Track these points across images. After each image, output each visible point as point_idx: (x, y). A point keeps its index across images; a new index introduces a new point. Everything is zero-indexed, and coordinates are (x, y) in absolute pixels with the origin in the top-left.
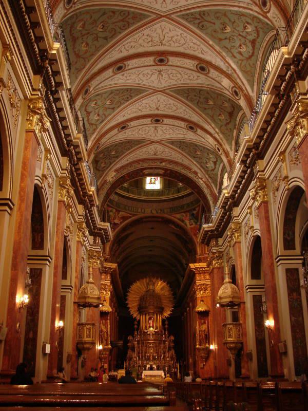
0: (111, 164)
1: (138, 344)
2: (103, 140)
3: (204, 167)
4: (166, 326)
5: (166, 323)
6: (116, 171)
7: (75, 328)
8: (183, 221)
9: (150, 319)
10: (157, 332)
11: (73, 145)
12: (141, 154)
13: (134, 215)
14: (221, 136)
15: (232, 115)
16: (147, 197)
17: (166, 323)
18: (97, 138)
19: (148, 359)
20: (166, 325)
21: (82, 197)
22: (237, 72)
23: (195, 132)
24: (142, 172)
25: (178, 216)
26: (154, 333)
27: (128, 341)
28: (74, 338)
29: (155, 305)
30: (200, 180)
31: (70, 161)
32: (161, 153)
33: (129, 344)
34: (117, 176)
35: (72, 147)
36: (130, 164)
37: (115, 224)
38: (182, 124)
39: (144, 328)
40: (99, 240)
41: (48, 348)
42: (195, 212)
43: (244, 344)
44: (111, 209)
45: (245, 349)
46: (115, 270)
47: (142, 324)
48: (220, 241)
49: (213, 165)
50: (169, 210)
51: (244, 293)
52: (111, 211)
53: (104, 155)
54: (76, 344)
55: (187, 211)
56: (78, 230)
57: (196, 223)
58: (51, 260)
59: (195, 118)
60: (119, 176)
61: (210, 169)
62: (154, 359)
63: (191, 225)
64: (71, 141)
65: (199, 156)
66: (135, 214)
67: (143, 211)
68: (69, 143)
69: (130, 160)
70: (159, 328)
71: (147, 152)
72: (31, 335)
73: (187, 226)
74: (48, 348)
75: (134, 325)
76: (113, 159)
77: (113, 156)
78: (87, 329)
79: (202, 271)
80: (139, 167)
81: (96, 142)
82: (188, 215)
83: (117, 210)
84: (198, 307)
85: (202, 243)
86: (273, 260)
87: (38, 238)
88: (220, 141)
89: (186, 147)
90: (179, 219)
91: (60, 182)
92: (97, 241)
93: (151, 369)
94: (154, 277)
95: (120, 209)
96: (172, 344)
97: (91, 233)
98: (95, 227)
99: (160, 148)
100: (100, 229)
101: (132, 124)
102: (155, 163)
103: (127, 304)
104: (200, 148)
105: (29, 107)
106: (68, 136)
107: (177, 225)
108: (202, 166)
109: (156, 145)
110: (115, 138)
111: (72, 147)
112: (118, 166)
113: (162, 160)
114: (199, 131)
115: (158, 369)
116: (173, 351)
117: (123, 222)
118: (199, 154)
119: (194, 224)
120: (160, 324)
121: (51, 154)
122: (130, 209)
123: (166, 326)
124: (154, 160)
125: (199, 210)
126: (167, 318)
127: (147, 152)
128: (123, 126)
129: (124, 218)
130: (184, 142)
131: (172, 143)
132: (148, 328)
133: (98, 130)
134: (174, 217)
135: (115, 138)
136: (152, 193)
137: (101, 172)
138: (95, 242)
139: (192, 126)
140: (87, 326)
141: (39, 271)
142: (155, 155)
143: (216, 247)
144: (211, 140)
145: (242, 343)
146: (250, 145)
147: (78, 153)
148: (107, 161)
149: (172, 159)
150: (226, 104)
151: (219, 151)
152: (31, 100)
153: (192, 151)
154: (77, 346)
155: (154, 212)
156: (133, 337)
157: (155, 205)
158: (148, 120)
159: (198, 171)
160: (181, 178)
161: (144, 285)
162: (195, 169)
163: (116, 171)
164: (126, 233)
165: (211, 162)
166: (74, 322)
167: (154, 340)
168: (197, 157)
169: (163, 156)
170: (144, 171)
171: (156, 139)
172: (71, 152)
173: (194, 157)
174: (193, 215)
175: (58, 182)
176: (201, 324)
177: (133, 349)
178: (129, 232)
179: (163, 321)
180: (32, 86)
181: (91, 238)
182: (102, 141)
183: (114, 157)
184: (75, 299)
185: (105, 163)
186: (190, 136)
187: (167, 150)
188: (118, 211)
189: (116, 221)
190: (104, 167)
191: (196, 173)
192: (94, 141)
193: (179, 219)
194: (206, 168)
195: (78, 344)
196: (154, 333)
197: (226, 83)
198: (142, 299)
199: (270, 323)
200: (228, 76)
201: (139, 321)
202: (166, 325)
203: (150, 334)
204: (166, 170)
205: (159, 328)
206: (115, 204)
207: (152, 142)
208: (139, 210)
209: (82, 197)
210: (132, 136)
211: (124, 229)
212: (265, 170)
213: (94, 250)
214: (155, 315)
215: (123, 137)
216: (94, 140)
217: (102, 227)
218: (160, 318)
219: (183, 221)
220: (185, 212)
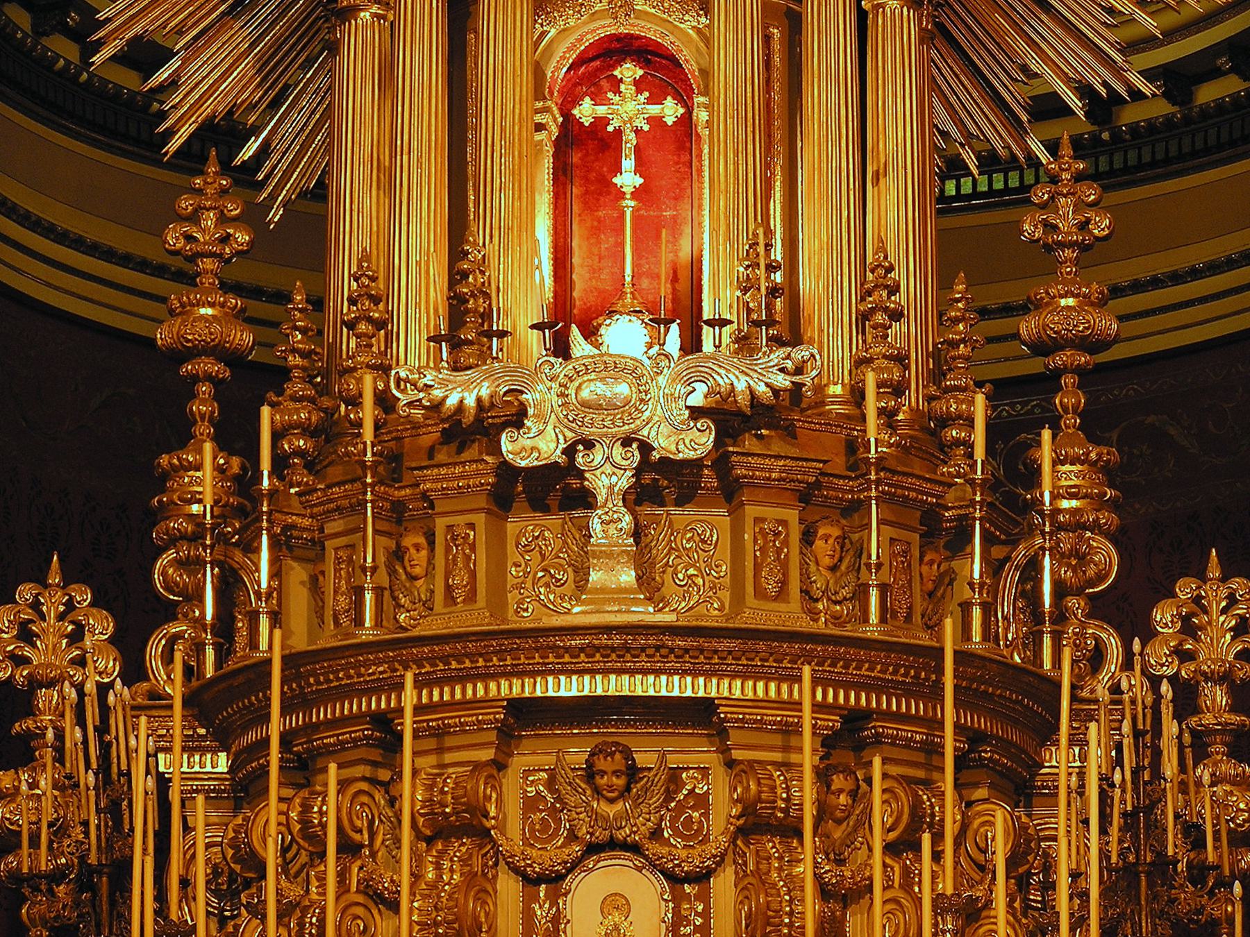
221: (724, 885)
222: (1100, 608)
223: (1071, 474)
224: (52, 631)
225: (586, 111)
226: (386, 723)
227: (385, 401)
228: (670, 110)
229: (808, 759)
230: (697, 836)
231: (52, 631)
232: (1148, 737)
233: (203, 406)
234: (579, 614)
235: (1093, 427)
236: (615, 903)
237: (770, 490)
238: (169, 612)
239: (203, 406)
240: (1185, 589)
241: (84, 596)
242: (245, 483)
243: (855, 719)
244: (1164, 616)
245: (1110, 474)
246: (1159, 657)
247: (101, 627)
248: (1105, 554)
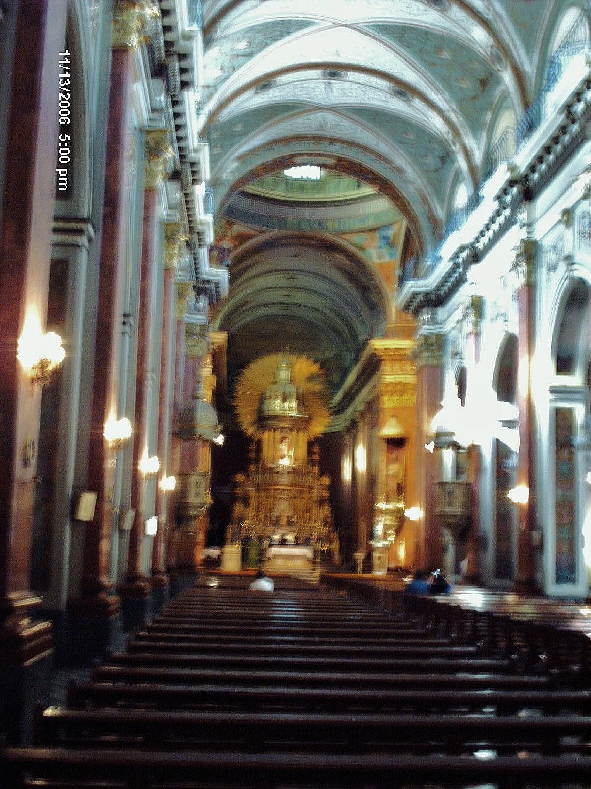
4: (316, 457)
8: (362, 249)
9: (282, 440)
15: (484, 83)
17: (316, 449)
19: (276, 523)
22: (505, 20)
23: (407, 101)
33: (239, 491)
38: (384, 84)
40: (203, 302)
47: (266, 452)
48: (441, 312)
57: (391, 255)
59: (410, 76)
62: (289, 523)
63: (379, 258)
75: (249, 451)
79: (398, 356)
84: (383, 424)
85: (407, 307)
93: (283, 543)
96: (326, 494)
99: (331, 118)
100: (208, 281)
101: (284, 78)
103: (233, 408)
110: (246, 104)
112: (246, 148)
113: (333, 140)
114: (417, 102)
115: (297, 543)
117: (241, 244)
120: (303, 451)
124: (318, 139)
125: (400, 229)
128: (264, 83)
135: (246, 104)
136: (303, 184)
139: (403, 89)
150: (477, 66)
158: (316, 73)
163: (242, 158)
164: (243, 265)
167: (292, 485)
174: (385, 238)
176: (389, 462)
177: (246, 501)
178: (248, 262)
179: (310, 444)
186: (397, 105)
191: (400, 170)
193: (354, 244)
197: (479, 35)
199: (519, 495)
200: (485, 23)
204: (340, 160)
207: (317, 108)
218: (303, 439)
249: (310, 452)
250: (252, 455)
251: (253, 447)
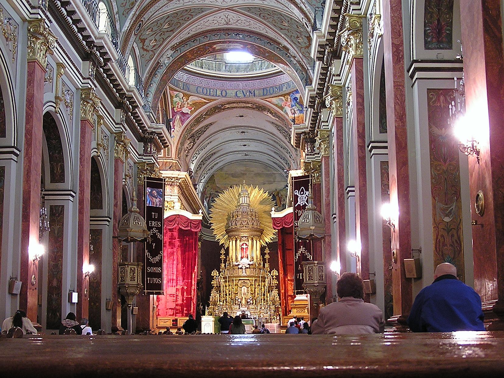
0: (164, 40)
1: (226, 282)
2: (146, 16)
3: (296, 43)
4: (267, 256)
5: (267, 251)
6: (173, 48)
7: (116, 269)
8: (282, 108)
10: (252, 265)
11: (96, 46)
12: (206, 24)
13: (210, 100)
14: (308, 8)
16: (229, 73)
17: (267, 251)
18: (137, 13)
20: (266, 254)
21: (119, 99)
24: (211, 47)
25: (274, 100)
26: (248, 266)
27: (212, 278)
28: (114, 282)
29: (250, 226)
30: (292, 59)
31: (94, 64)
32: (235, 21)
34: (176, 55)
35: (95, 49)
36: (194, 38)
37: (183, 114)
39: (234, 260)
41: (75, 296)
42: (298, 96)
43: (328, 288)
44: (176, 93)
45: (328, 292)
46: (185, 181)
47: (232, 253)
49: (306, 40)
50: (261, 92)
51: (330, 223)
52: (176, 96)
53: (152, 31)
54: (117, 289)
55: (289, 94)
56: (115, 143)
58: (74, 194)
60: (178, 54)
61: (304, 45)
64: (93, 42)
65: (287, 28)
66: (213, 98)
67: (224, 94)
68: (90, 44)
69: (192, 33)
70: (255, 260)
71: (215, 22)
72: (55, 283)
73: (288, 115)
74: (75, 296)
76: (167, 34)
77: (166, 30)
78: (131, 269)
80: (206, 41)
81: (137, 18)
82: (289, 100)
83: (185, 95)
86: (343, 190)
87: (57, 169)
88: (308, 14)
89: (269, 15)
90: (274, 104)
91: (82, 95)
92: (149, 149)
94: (249, 185)
95: (189, 93)
97: (141, 139)
98: (144, 131)
99: (232, 15)
100: (152, 133)
102: (229, 35)
104: (286, 18)
105: (29, 30)
106: (86, 38)
107: (275, 114)
108: (292, 41)
109: (227, 13)
110: (164, 9)
111: (95, 49)
112: (176, 41)
116: (275, 292)
117: (196, 110)
118: (286, 25)
119: (298, 112)
120: (257, 253)
121: (64, 67)
122: (205, 91)
123: (267, 256)
126: (269, 245)
127: (215, 22)
129: (197, 105)
130: (264, 9)
131: (249, 9)
132: (239, 259)
133: (137, 4)
134: (268, 101)
137: (151, 53)
138: (145, 151)
140: (130, 266)
141: (60, 209)
142: (227, 24)
143: (311, 155)
144: (296, 11)
145: (326, 287)
146: (322, 42)
147: (103, 54)
148: (158, 37)
149: (254, 29)
151: (308, 28)
152: (30, 22)
153: (277, 21)
154: (119, 292)
155: (240, 94)
156: (220, 272)
157: (241, 84)
159: (289, 46)
160: (267, 55)
161: (234, 195)
162: (286, 44)
163: (173, 48)
165: (304, 37)
166: (114, 262)
168: (285, 29)
169: (239, 26)
170: (215, 46)
171: (225, 5)
172: (95, 55)
173: (281, 29)
174: (296, 99)
175: (80, 95)
179: (262, 249)
180: (30, 5)
181: (140, 146)
182: (144, 17)
183: (168, 31)
184: (114, 233)
185: (155, 40)
187: (243, 18)
188: (188, 96)
189: (185, 110)
190: (154, 46)
192: (134, 19)
193: (276, 105)
194: (298, 44)
195: (119, 289)
196: (248, 266)
198: (230, 217)
201: (227, 250)
202: (266, 254)
203: (241, 268)
205: (255, 260)
206: (181, 85)
208: (219, 93)
209: (119, 99)
210: (190, 3)
211: (198, 120)
212: (340, 74)
213: (145, 162)
214: (250, 241)
215: (176, 6)
216: (133, 17)
217: (154, 130)
219: (282, 108)
220: (284, 95)
221: (249, 288)
222: (268, 272)
223: (267, 265)
224: (215, 273)
225: (242, 247)
226: (233, 280)
227: (233, 264)
228: (247, 247)
229: (254, 281)
230: (248, 285)
231: (215, 273)
232: (270, 280)
233: (223, 261)
234: (242, 275)
235: (268, 263)
236: (244, 289)
237: (252, 268)
238: (221, 272)
239: (223, 261)
240: (273, 270)
241: (217, 271)
242: (225, 265)
243: (256, 280)
244: (272, 272)
245: (269, 265)
246: (271, 274)
247: (218, 273)
248: (269, 269)
249: (263, 254)
250: (223, 257)
251: (223, 252)
